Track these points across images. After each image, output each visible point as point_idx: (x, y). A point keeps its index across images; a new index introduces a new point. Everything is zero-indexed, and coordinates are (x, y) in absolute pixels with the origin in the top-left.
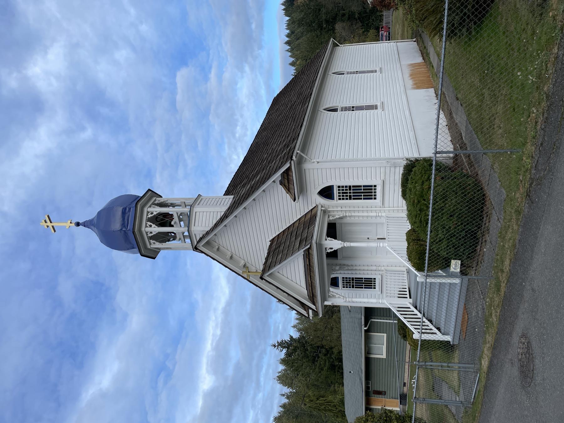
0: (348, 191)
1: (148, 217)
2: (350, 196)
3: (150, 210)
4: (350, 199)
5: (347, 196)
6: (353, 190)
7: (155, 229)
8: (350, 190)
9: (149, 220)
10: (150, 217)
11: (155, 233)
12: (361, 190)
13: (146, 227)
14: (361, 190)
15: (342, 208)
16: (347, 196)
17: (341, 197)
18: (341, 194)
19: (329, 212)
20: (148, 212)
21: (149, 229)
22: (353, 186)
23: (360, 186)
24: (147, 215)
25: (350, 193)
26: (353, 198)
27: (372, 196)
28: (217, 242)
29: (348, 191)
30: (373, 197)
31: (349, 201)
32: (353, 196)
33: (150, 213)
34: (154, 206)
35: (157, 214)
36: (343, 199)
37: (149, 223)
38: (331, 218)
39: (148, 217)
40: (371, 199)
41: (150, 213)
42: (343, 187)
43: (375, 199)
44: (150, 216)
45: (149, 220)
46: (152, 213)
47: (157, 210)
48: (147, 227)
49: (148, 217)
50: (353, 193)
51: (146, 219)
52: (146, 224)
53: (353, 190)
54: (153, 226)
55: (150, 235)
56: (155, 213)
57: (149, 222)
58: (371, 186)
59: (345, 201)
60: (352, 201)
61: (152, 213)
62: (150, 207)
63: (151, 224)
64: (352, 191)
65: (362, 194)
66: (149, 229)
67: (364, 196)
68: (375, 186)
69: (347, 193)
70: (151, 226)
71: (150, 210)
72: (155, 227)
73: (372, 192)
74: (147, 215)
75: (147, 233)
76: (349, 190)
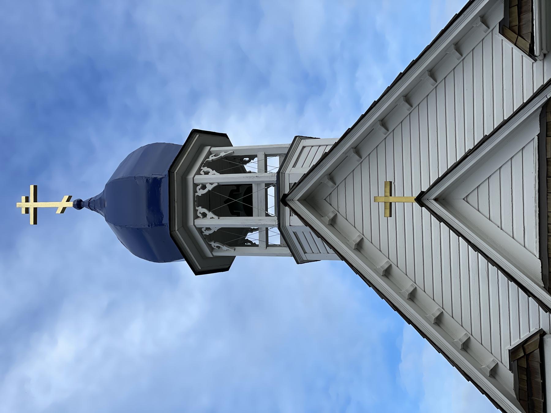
1: (196, 194)
9: (201, 201)
10: (200, 195)
13: (196, 217)
20: (195, 185)
24: (195, 191)
28: (334, 204)
33: (199, 187)
35: (214, 189)
37: (201, 210)
41: (199, 187)
44: (200, 192)
45: (201, 201)
46: (204, 187)
48: (198, 217)
49: (198, 196)
51: (194, 201)
52: (195, 211)
54: (210, 214)
56: (209, 188)
57: (200, 207)
61: (204, 187)
62: (198, 173)
66: (201, 222)
70: (204, 215)
71: (201, 179)
72: (212, 218)
74: (195, 191)
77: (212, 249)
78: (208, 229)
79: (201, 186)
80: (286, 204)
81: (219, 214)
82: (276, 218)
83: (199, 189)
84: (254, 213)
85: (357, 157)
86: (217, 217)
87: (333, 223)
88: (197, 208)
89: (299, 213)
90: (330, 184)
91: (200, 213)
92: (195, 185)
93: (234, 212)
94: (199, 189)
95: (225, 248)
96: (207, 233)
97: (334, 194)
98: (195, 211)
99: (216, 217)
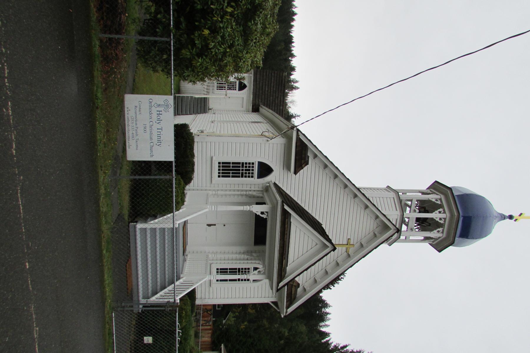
1: (443, 229)
4: (239, 269)
7: (435, 215)
13: (445, 219)
20: (443, 233)
21: (443, 216)
24: (443, 230)
31: (241, 267)
34: (436, 238)
36: (245, 269)
37: (442, 222)
39: (443, 229)
46: (438, 231)
49: (442, 227)
51: (444, 226)
52: (445, 221)
54: (438, 220)
56: (435, 231)
57: (442, 223)
59: (244, 267)
62: (439, 238)
63: (439, 221)
66: (443, 216)
70: (440, 219)
74: (443, 230)
75: (444, 212)
77: (441, 199)
78: (440, 212)
79: (440, 232)
80: (397, 228)
81: (432, 219)
82: (404, 216)
83: (441, 231)
84: (415, 220)
85: (363, 243)
87: (377, 217)
88: (444, 222)
89: (392, 224)
90: (376, 233)
91: (442, 220)
93: (425, 220)
94: (441, 231)
95: (434, 200)
96: (441, 210)
97: (375, 228)
98: (445, 221)
99: (434, 218)
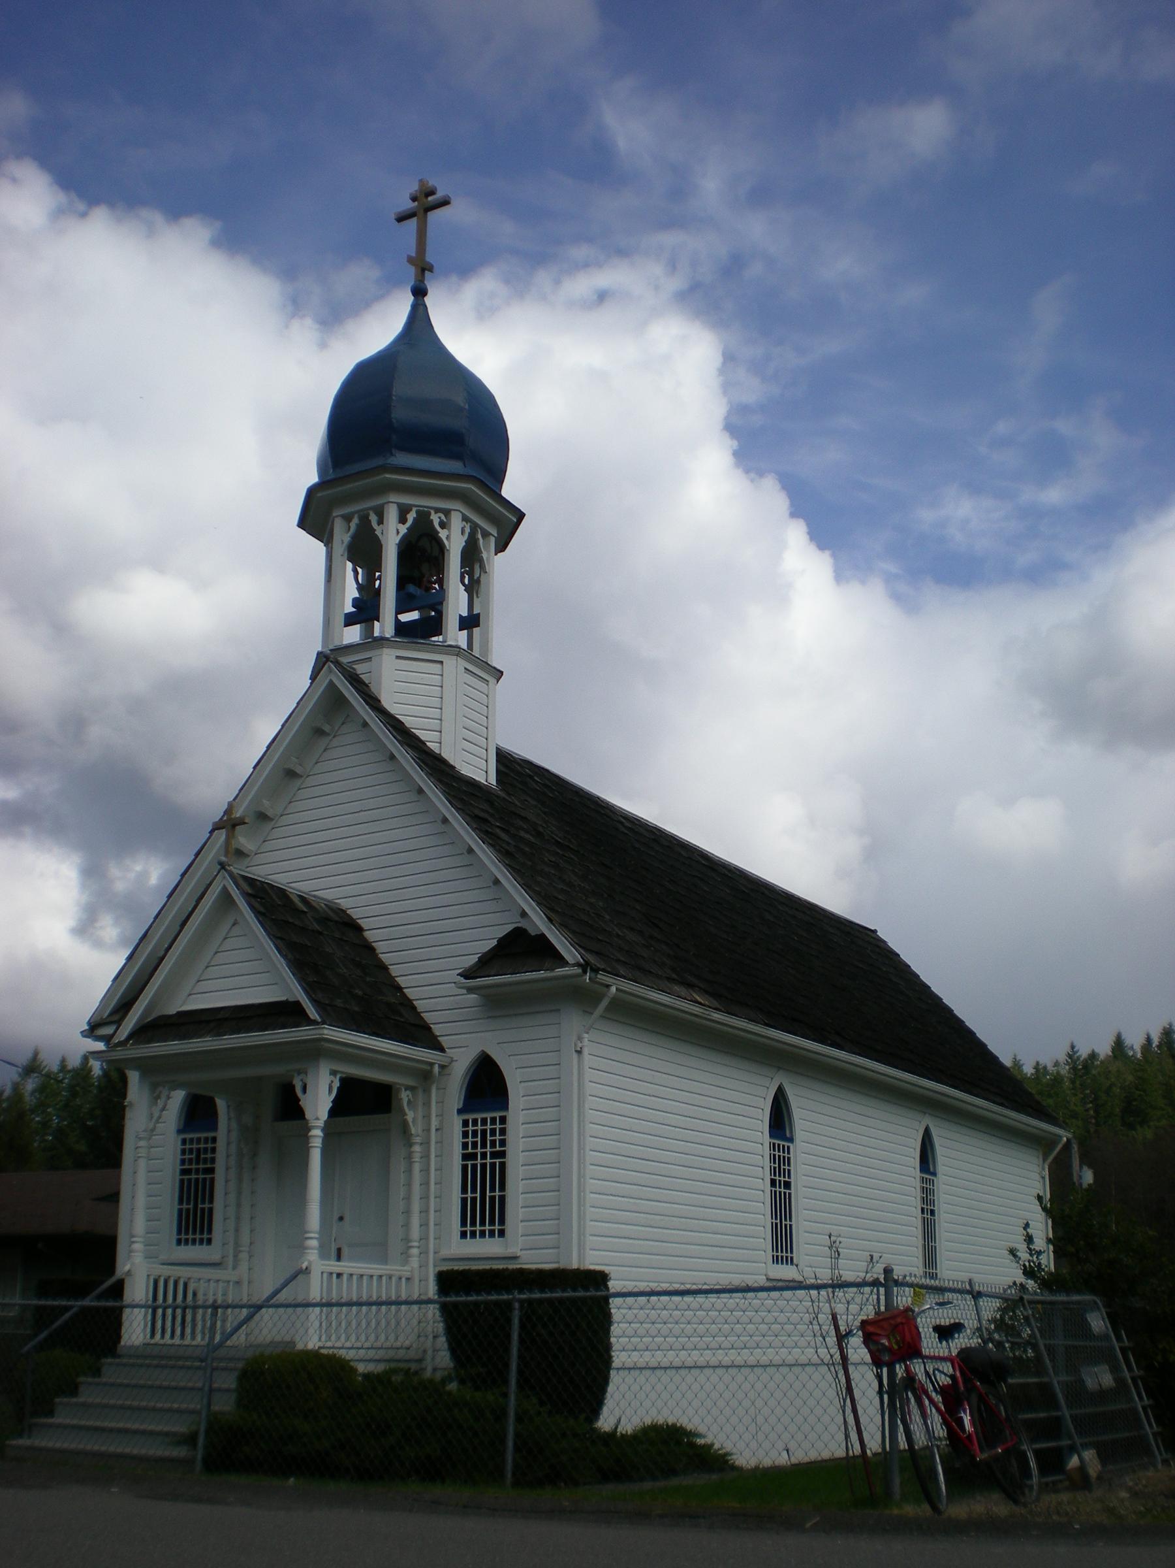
0: (488, 1149)
1: (433, 512)
2: (473, 1156)
3: (456, 522)
4: (465, 1157)
5: (475, 1145)
6: (493, 1165)
7: (392, 534)
8: (494, 1155)
9: (423, 518)
10: (431, 518)
11: (378, 533)
12: (493, 1189)
14: (493, 1189)
15: (437, 1130)
16: (475, 1145)
17: (471, 1128)
18: (479, 1127)
19: (424, 1091)
20: (447, 513)
21: (392, 514)
22: (503, 1166)
23: (503, 1187)
24: (437, 510)
25: (484, 1156)
26: (467, 1165)
27: (473, 1224)
29: (488, 1149)
30: (469, 1228)
32: (474, 1167)
34: (468, 530)
36: (465, 1134)
37: (411, 517)
38: (405, 1096)
39: (433, 512)
40: (464, 1223)
41: (443, 517)
42: (503, 1132)
43: (463, 1235)
44: (435, 518)
45: (423, 518)
47: (454, 541)
49: (430, 514)
50: (484, 1166)
53: (493, 1165)
54: (403, 529)
55: (373, 519)
56: (443, 534)
58: (502, 1221)
60: (457, 1162)
61: (443, 525)
62: (465, 519)
63: (408, 524)
64: (488, 1160)
65: (478, 1195)
66: (392, 514)
67: (474, 1200)
68: (502, 1233)
69: (484, 1145)
70: (403, 520)
71: (456, 522)
72: (398, 533)
73: (483, 1223)
74: (437, 510)
76: (491, 1153)
79: (445, 520)
83: (440, 518)
86: (397, 542)
92: (447, 513)
99: (397, 539)
